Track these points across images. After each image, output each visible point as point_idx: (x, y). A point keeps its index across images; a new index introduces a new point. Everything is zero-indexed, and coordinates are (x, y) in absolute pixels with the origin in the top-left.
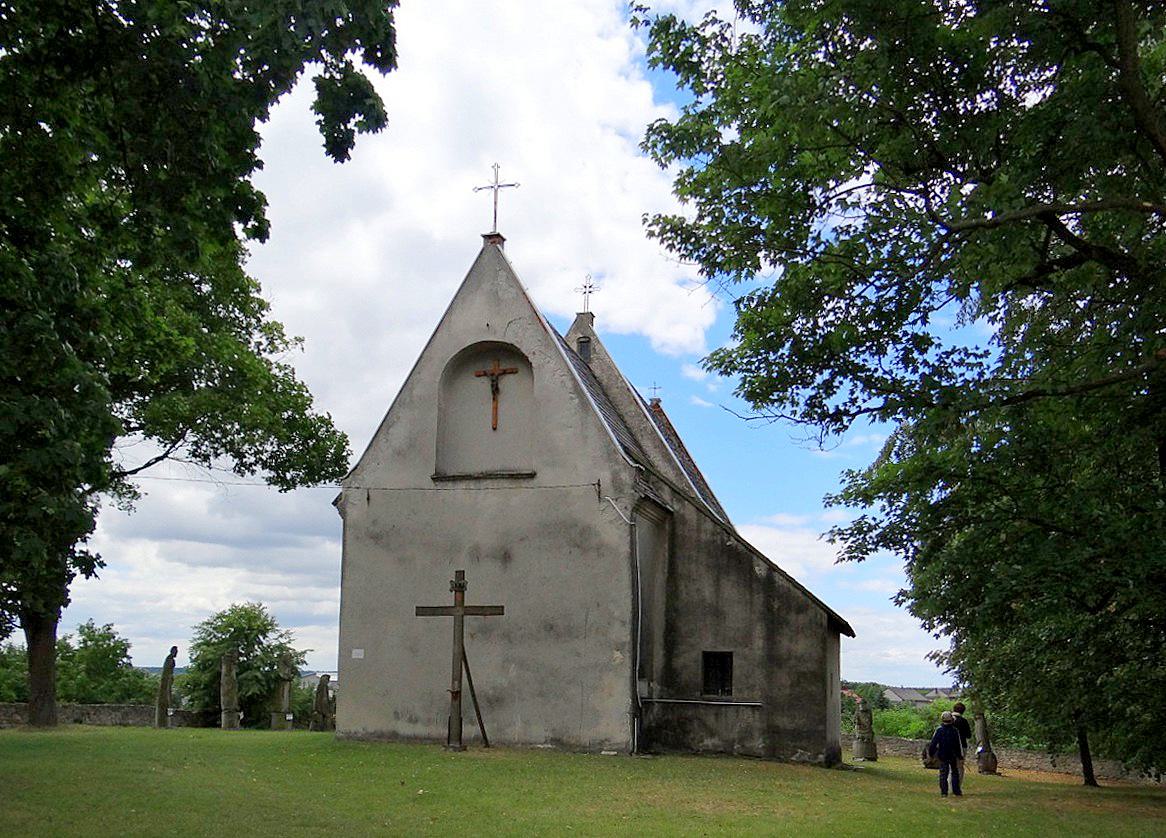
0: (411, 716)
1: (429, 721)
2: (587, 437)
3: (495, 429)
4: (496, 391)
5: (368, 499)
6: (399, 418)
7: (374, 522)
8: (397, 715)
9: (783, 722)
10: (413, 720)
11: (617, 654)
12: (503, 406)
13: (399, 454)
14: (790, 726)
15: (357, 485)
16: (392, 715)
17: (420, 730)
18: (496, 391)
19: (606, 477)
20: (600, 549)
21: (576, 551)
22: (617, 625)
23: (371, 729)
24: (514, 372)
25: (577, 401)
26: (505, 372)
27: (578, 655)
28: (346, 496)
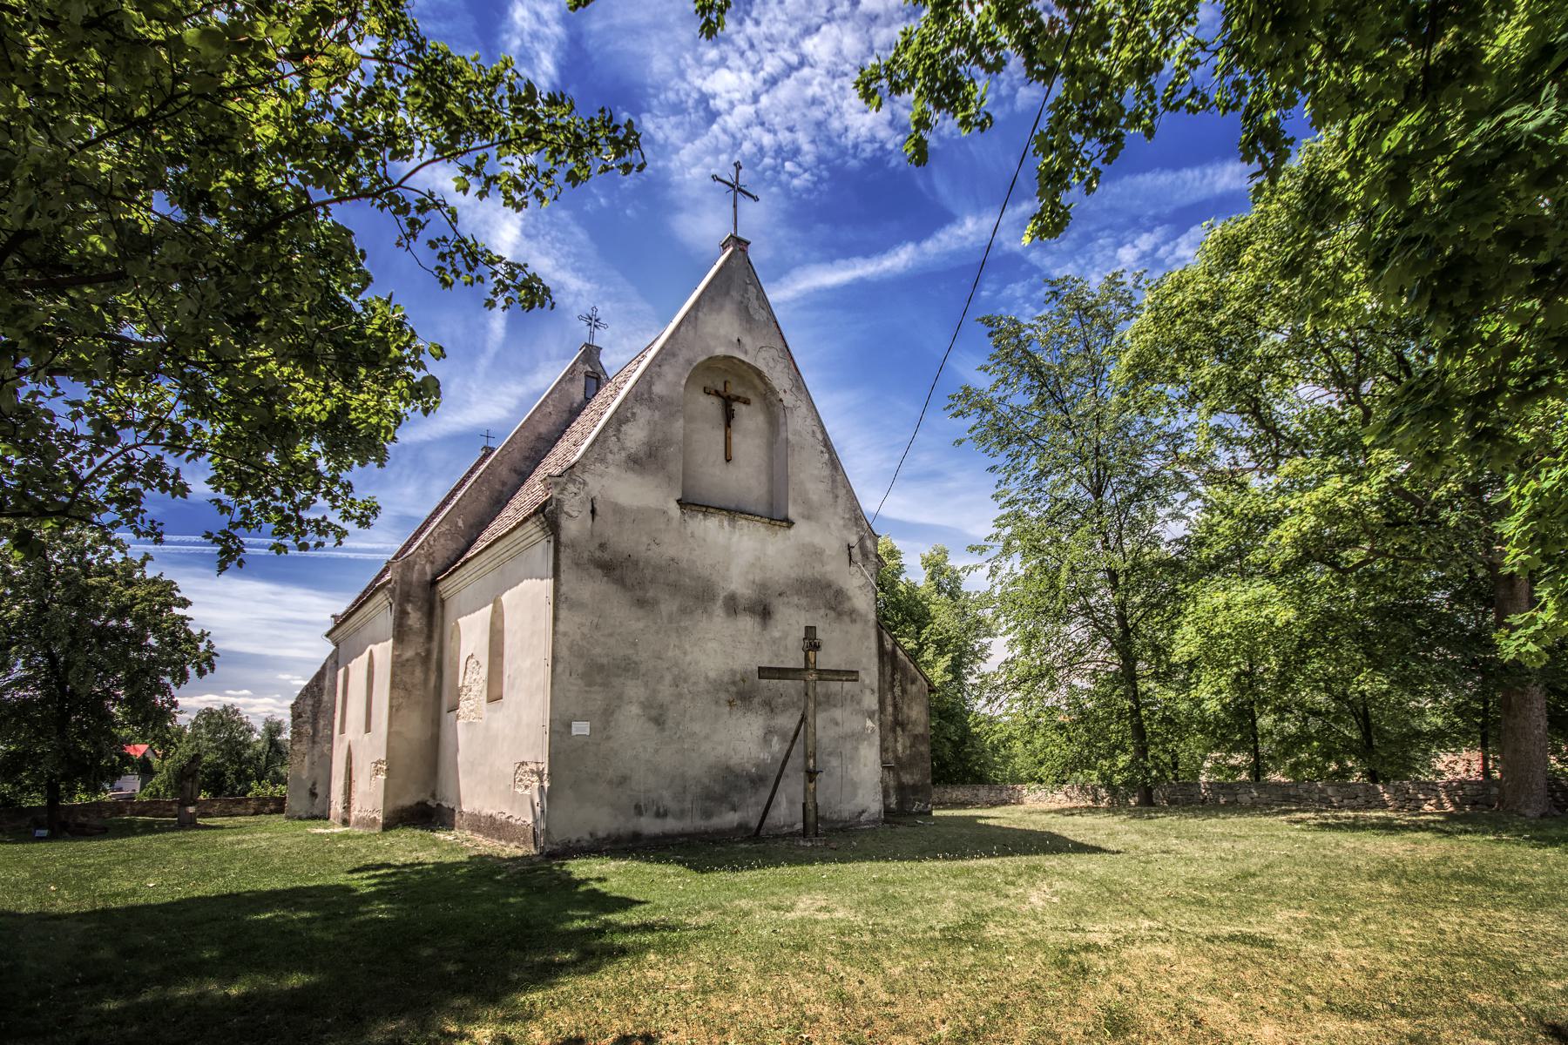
0: (658, 808)
1: (682, 814)
2: (837, 497)
3: (728, 460)
4: (729, 417)
5: (593, 511)
6: (634, 414)
7: (602, 546)
8: (639, 810)
9: (907, 779)
10: (661, 814)
11: (869, 723)
12: (736, 439)
13: (635, 462)
14: (911, 782)
15: (575, 490)
16: (632, 811)
17: (671, 825)
18: (729, 417)
19: (854, 540)
20: (853, 615)
21: (832, 614)
22: (868, 692)
23: (601, 834)
24: (747, 402)
25: (827, 456)
26: (738, 399)
27: (837, 724)
28: (558, 500)
